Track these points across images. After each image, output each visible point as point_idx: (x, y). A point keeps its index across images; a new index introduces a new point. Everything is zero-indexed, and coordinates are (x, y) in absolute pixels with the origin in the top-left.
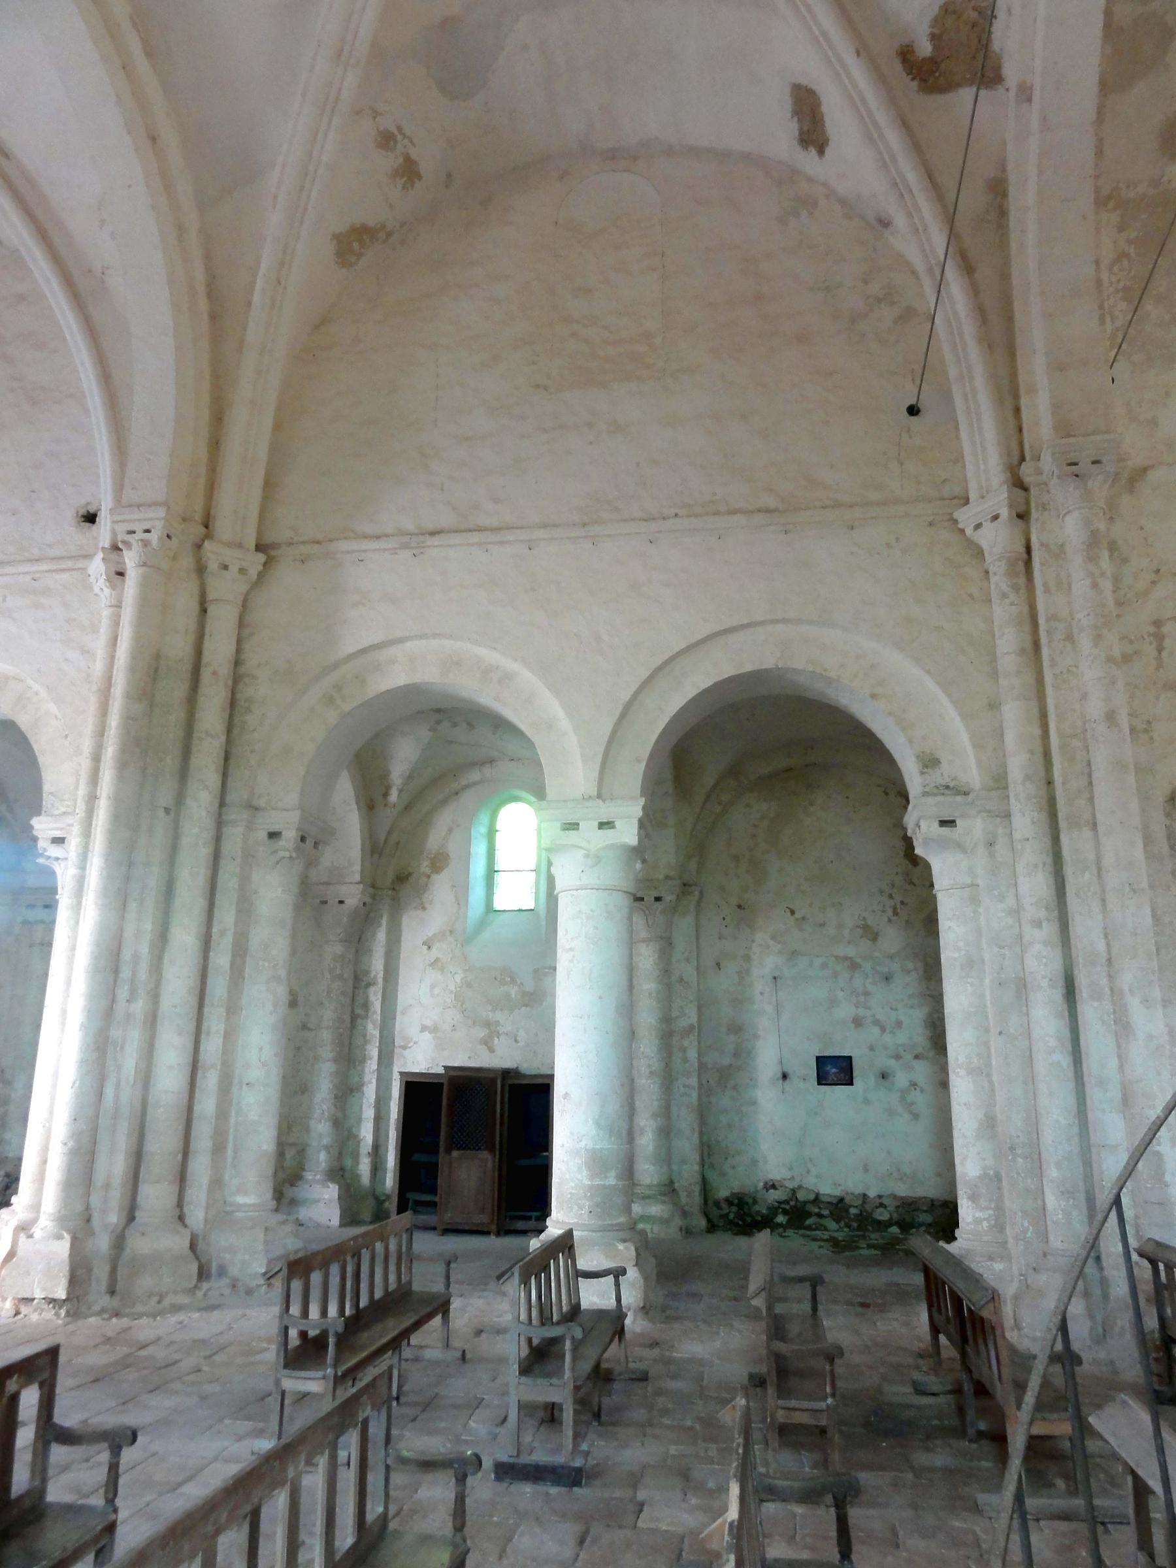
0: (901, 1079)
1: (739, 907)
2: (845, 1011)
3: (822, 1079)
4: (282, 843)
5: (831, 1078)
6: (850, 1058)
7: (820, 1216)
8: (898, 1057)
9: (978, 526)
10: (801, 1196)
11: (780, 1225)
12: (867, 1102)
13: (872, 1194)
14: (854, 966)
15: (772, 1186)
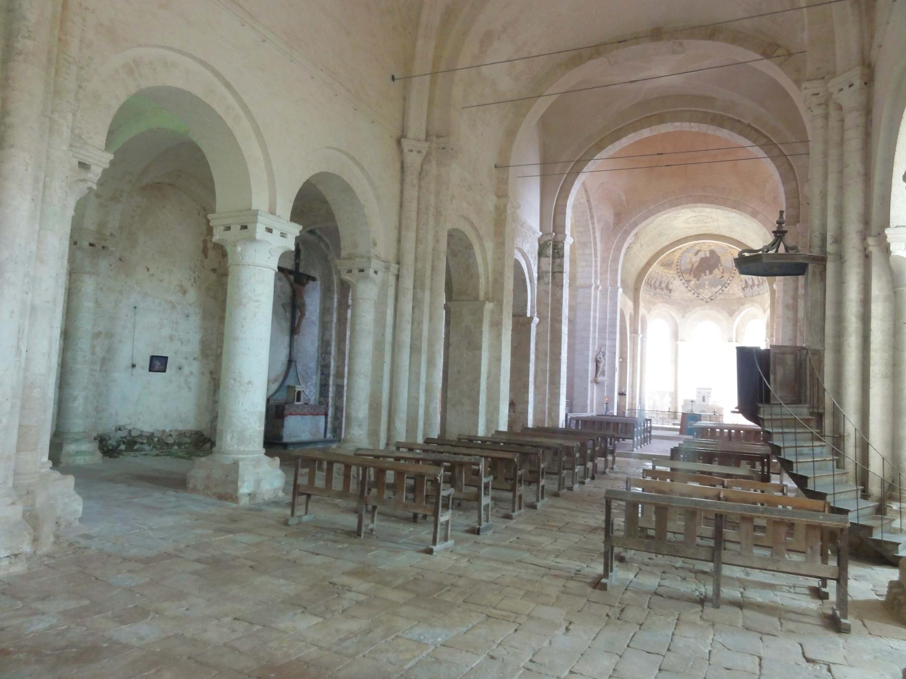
0: (186, 370)
1: (120, 259)
2: (166, 332)
3: (151, 369)
4: (90, 175)
5: (157, 368)
6: (166, 358)
7: (142, 443)
8: (186, 358)
9: (411, 151)
10: (134, 434)
11: (122, 451)
12: (171, 381)
13: (167, 430)
14: (173, 307)
15: (119, 429)
